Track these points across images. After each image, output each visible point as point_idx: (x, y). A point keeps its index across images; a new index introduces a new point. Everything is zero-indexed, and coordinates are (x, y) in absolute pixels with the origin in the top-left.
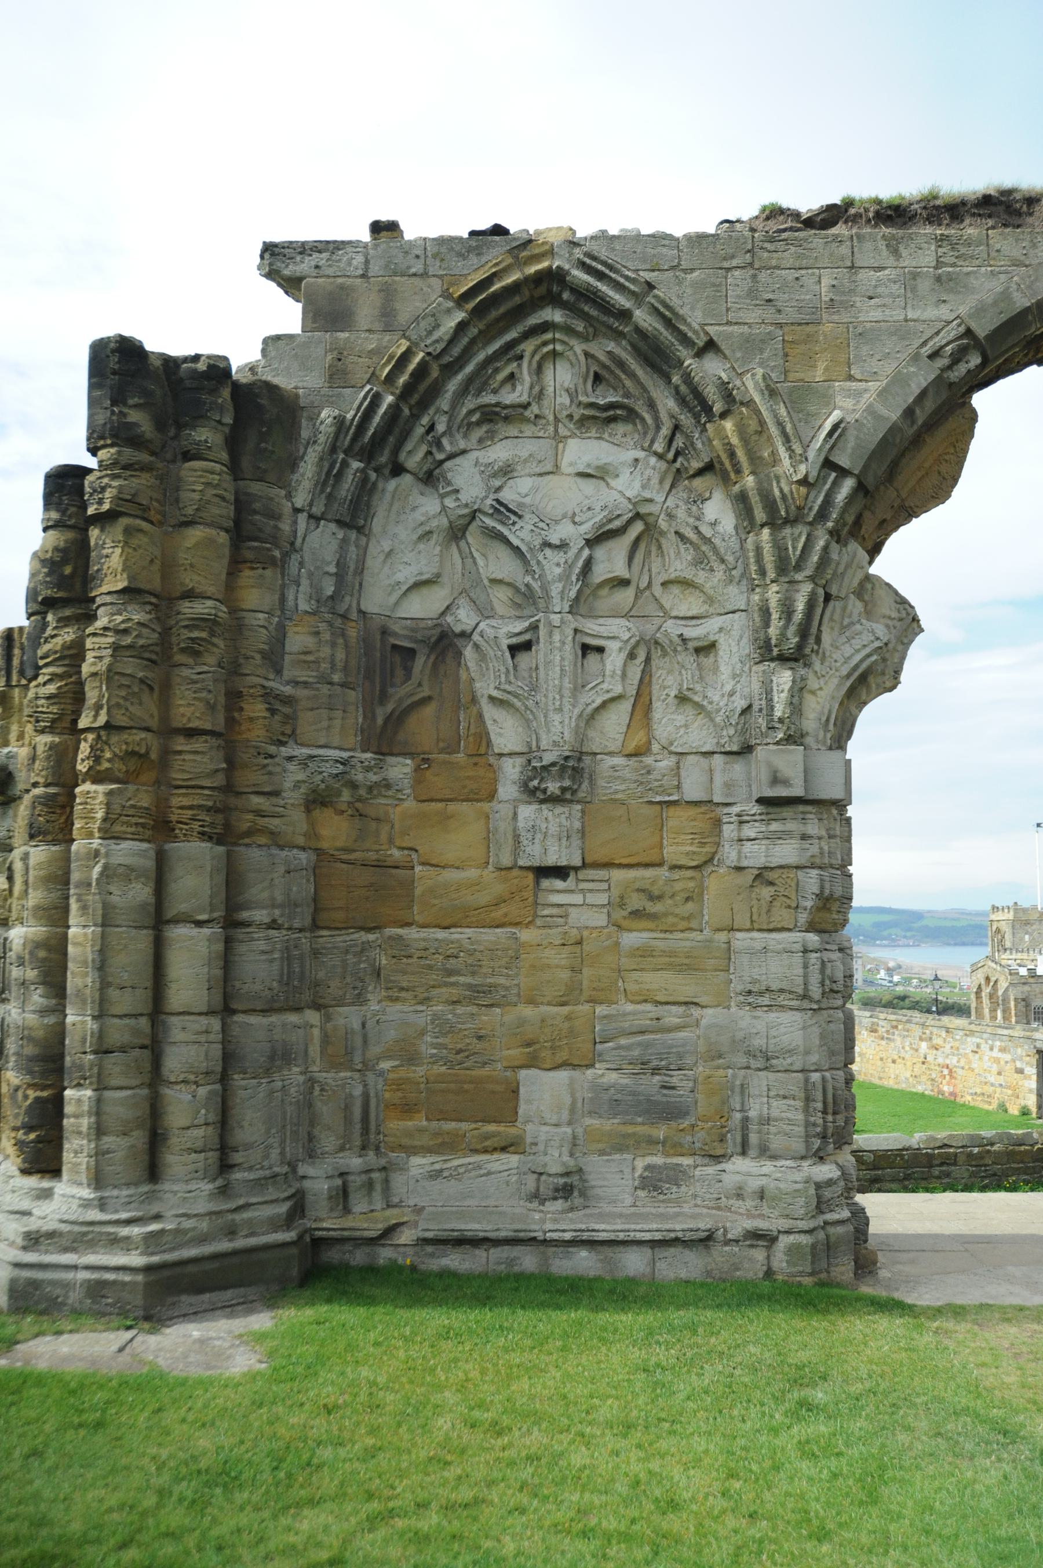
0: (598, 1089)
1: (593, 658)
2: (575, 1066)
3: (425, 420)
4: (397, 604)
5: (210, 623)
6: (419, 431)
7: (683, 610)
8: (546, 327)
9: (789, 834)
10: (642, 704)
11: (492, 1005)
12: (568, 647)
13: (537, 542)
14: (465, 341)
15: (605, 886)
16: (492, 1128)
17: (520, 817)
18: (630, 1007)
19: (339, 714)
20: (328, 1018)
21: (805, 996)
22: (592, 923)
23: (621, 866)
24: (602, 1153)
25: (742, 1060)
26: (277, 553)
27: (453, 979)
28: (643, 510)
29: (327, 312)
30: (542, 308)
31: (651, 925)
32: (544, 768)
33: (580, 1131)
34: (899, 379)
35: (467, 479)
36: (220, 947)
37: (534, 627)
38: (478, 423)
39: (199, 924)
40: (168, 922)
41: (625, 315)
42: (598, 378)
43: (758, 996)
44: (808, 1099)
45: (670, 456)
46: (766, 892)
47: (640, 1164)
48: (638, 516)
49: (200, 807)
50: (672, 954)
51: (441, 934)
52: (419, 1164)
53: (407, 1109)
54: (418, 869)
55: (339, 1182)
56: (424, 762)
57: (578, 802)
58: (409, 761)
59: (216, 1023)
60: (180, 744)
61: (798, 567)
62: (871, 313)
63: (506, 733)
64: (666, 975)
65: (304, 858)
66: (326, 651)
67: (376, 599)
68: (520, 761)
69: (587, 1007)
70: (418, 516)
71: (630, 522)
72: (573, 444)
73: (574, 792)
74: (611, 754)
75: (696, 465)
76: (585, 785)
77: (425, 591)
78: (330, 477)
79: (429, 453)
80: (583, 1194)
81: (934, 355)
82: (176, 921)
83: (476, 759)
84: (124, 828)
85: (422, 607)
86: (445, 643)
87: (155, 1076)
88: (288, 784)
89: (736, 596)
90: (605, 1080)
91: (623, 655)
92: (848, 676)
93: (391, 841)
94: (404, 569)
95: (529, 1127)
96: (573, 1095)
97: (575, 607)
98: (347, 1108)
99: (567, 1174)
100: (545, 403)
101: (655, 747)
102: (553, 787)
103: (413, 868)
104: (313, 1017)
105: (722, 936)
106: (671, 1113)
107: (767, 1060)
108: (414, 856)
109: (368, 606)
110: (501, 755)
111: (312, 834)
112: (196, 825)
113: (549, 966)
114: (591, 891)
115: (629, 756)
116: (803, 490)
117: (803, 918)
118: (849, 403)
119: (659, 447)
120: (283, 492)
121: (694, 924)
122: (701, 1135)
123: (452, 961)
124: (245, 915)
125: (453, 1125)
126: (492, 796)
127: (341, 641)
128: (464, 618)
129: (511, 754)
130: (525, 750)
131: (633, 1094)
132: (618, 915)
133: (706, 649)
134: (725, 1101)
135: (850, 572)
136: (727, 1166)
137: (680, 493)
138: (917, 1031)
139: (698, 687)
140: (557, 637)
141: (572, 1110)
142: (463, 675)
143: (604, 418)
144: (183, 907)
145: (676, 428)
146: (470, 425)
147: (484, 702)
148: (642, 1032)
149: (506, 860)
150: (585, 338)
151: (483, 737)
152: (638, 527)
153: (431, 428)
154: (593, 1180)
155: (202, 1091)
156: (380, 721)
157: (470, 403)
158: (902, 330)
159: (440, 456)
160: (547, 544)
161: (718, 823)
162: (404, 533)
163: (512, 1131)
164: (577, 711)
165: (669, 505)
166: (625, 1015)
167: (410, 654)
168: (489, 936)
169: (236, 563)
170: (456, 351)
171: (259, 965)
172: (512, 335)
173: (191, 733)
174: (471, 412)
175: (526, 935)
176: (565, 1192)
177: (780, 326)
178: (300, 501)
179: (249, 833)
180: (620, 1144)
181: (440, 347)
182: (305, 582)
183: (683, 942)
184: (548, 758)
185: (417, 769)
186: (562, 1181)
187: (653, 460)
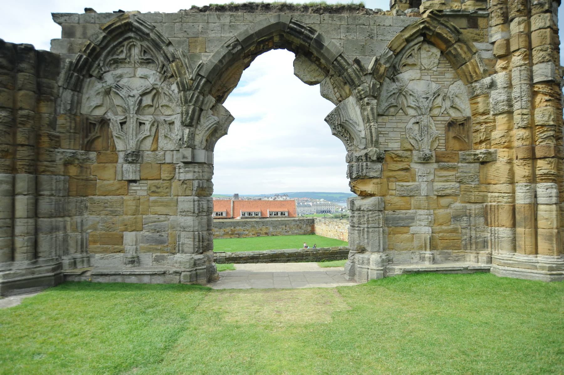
0: (144, 236)
1: (142, 126)
2: (137, 231)
3: (97, 63)
4: (92, 111)
5: (28, 117)
6: (96, 65)
7: (167, 113)
8: (130, 38)
9: (190, 171)
10: (156, 139)
12: (135, 123)
13: (127, 95)
14: (106, 41)
16: (116, 246)
18: (152, 216)
19: (73, 140)
20: (72, 219)
21: (194, 213)
23: (150, 180)
24: (144, 252)
25: (179, 229)
26: (53, 98)
28: (155, 87)
29: (68, 32)
30: (129, 32)
31: (157, 195)
33: (138, 247)
34: (218, 52)
35: (109, 78)
37: (126, 118)
38: (114, 63)
39: (25, 195)
41: (148, 35)
42: (145, 52)
43: (184, 213)
44: (194, 239)
45: (163, 72)
46: (185, 186)
47: (154, 255)
48: (154, 89)
49: (25, 165)
50: (162, 202)
51: (103, 197)
52: (98, 256)
53: (95, 242)
55: (73, 260)
56: (99, 153)
60: (20, 148)
61: (190, 101)
62: (212, 35)
63: (120, 145)
64: (161, 207)
66: (69, 124)
67: (85, 110)
68: (124, 152)
70: (96, 88)
71: (152, 90)
72: (139, 69)
73: (137, 161)
74: (147, 151)
75: (169, 75)
77: (99, 108)
78: (69, 77)
79: (99, 72)
81: (228, 47)
85: (99, 112)
86: (104, 122)
87: (13, 235)
88: (58, 158)
89: (179, 110)
91: (150, 125)
92: (208, 130)
93: (90, 174)
94: (92, 102)
96: (136, 238)
97: (137, 112)
98: (77, 242)
99: (133, 258)
100: (132, 58)
101: (159, 149)
102: (130, 159)
105: (176, 198)
106: (162, 242)
107: (184, 229)
109: (82, 112)
112: (24, 170)
116: (192, 82)
117: (194, 192)
118: (204, 59)
119: (159, 70)
120: (55, 82)
121: (168, 194)
122: (169, 248)
124: (42, 193)
125: (106, 246)
126: (117, 162)
127: (73, 121)
128: (110, 115)
129: (122, 151)
131: (152, 237)
132: (149, 192)
133: (172, 123)
134: (176, 239)
135: (208, 103)
136: (175, 256)
137: (166, 82)
138: (335, 223)
139: (169, 133)
140: (132, 120)
141: (136, 241)
142: (110, 130)
143: (148, 62)
145: (164, 66)
146: (111, 64)
147: (114, 138)
149: (120, 178)
150: (140, 41)
151: (114, 146)
152: (154, 91)
153: (99, 65)
155: (26, 238)
156: (85, 142)
157: (110, 58)
158: (220, 40)
159: (102, 72)
160: (129, 96)
161: (175, 168)
162: (92, 92)
163: (122, 247)
164: (137, 140)
165: (163, 86)
167: (95, 125)
168: (115, 198)
169: (38, 101)
170: (104, 44)
171: (45, 205)
172: (121, 40)
173: (23, 145)
174: (110, 61)
175: (125, 197)
176: (132, 262)
177: (188, 38)
178: (60, 83)
179: (43, 171)
181: (99, 43)
182: (62, 105)
183: (165, 199)
187: (158, 74)
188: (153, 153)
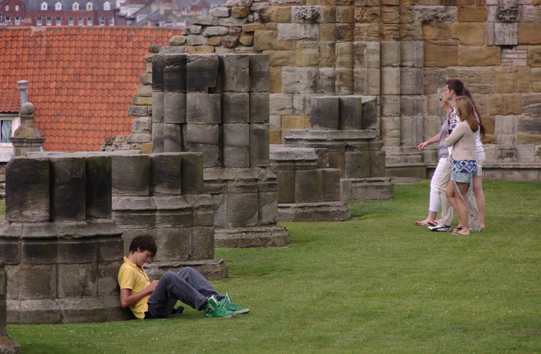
2: (514, 114)
11: (485, 93)
15: (526, 51)
17: (496, 28)
18: (534, 94)
20: (429, 98)
22: (521, 65)
23: (532, 44)
24: (524, 143)
27: (472, 84)
32: (504, 11)
33: (516, 136)
36: (399, 74)
39: (394, 67)
40: (384, 66)
49: (393, 30)
51: (468, 69)
54: (459, 46)
57: (517, 22)
58: (456, 8)
59: (398, 97)
60: (386, 9)
65: (421, 43)
69: (519, 94)
73: (515, 19)
74: (528, 4)
76: (519, 16)
80: (516, 156)
82: (386, 66)
83: (480, 7)
84: (372, 38)
88: (416, 19)
90: (525, 119)
95: (499, 135)
96: (514, 124)
99: (511, 149)
103: (457, 46)
104: (424, 97)
108: (458, 41)
110: (489, 5)
111: (424, 35)
112: (392, 36)
113: (505, 80)
114: (521, 53)
115: (535, 5)
123: (472, 78)
126: (486, 20)
129: (492, 5)
130: (498, 3)
131: (535, 123)
132: (530, 62)
141: (513, 129)
144: (389, 62)
148: (538, 102)
149: (491, 43)
154: (521, 152)
163: (492, 136)
166: (532, 96)
175: (498, 69)
176: (511, 155)
179: (406, 36)
180: (530, 141)
184: (506, 7)
185: (459, 11)
186: (509, 151)
188: (536, 8)
